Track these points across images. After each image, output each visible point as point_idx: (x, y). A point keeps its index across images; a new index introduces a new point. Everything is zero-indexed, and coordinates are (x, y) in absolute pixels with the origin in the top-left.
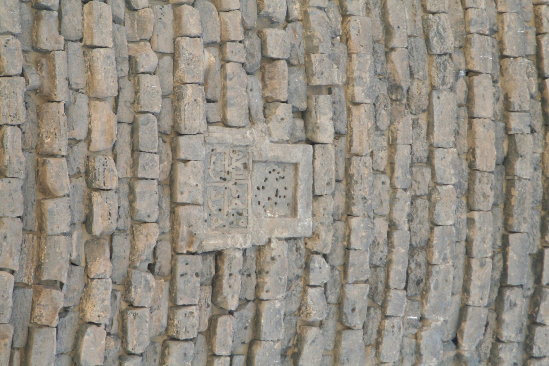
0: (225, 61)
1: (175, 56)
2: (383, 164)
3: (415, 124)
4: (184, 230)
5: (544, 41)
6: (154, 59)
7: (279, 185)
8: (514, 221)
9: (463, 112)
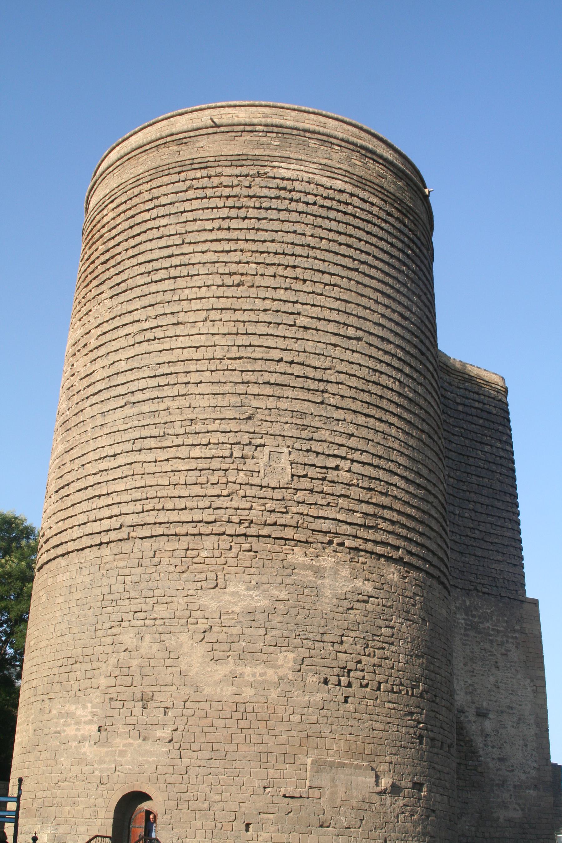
0: (242, 470)
1: (241, 484)
2: (271, 424)
3: (260, 413)
4: (286, 486)
5: (238, 369)
6: (241, 491)
7: (275, 456)
8: (288, 384)
9: (257, 397)
